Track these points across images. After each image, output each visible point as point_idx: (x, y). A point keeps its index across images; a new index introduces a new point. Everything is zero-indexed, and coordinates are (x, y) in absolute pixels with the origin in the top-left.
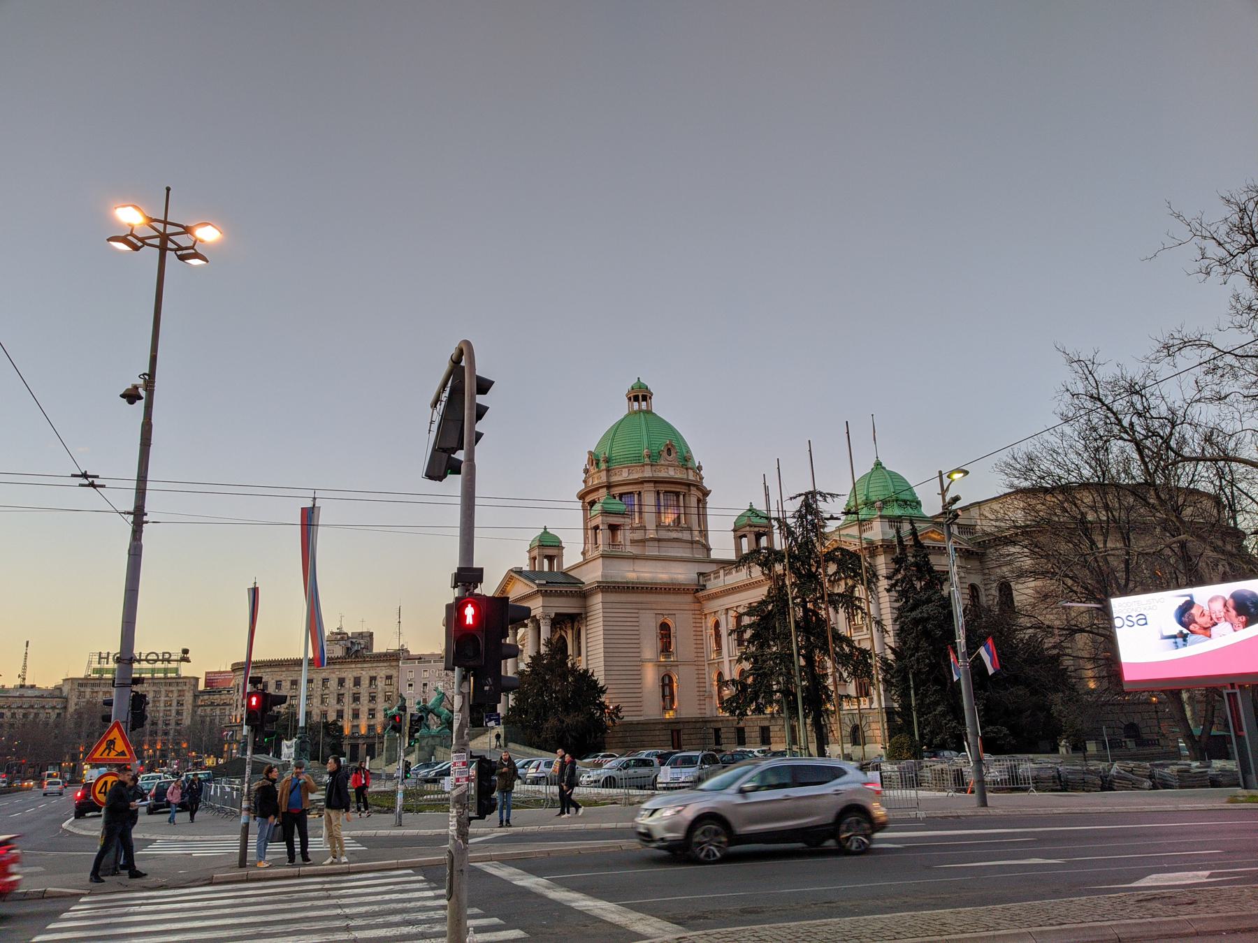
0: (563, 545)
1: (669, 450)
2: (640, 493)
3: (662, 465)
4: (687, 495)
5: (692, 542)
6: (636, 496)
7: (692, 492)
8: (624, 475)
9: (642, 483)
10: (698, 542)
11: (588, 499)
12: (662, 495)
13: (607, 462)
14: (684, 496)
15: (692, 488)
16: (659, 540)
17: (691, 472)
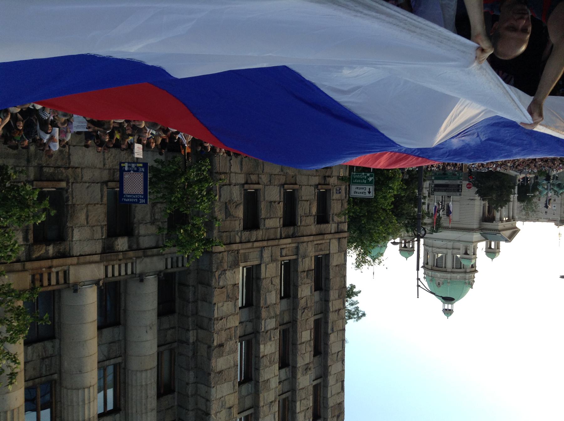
0: (485, 253)
1: (439, 285)
2: (453, 268)
3: (443, 278)
4: (433, 266)
5: (432, 247)
6: (454, 267)
7: (430, 267)
8: (458, 276)
9: (452, 272)
10: (430, 247)
11: (473, 269)
12: (444, 266)
13: (465, 283)
14: (434, 265)
15: (430, 268)
16: (446, 248)
17: (430, 275)
